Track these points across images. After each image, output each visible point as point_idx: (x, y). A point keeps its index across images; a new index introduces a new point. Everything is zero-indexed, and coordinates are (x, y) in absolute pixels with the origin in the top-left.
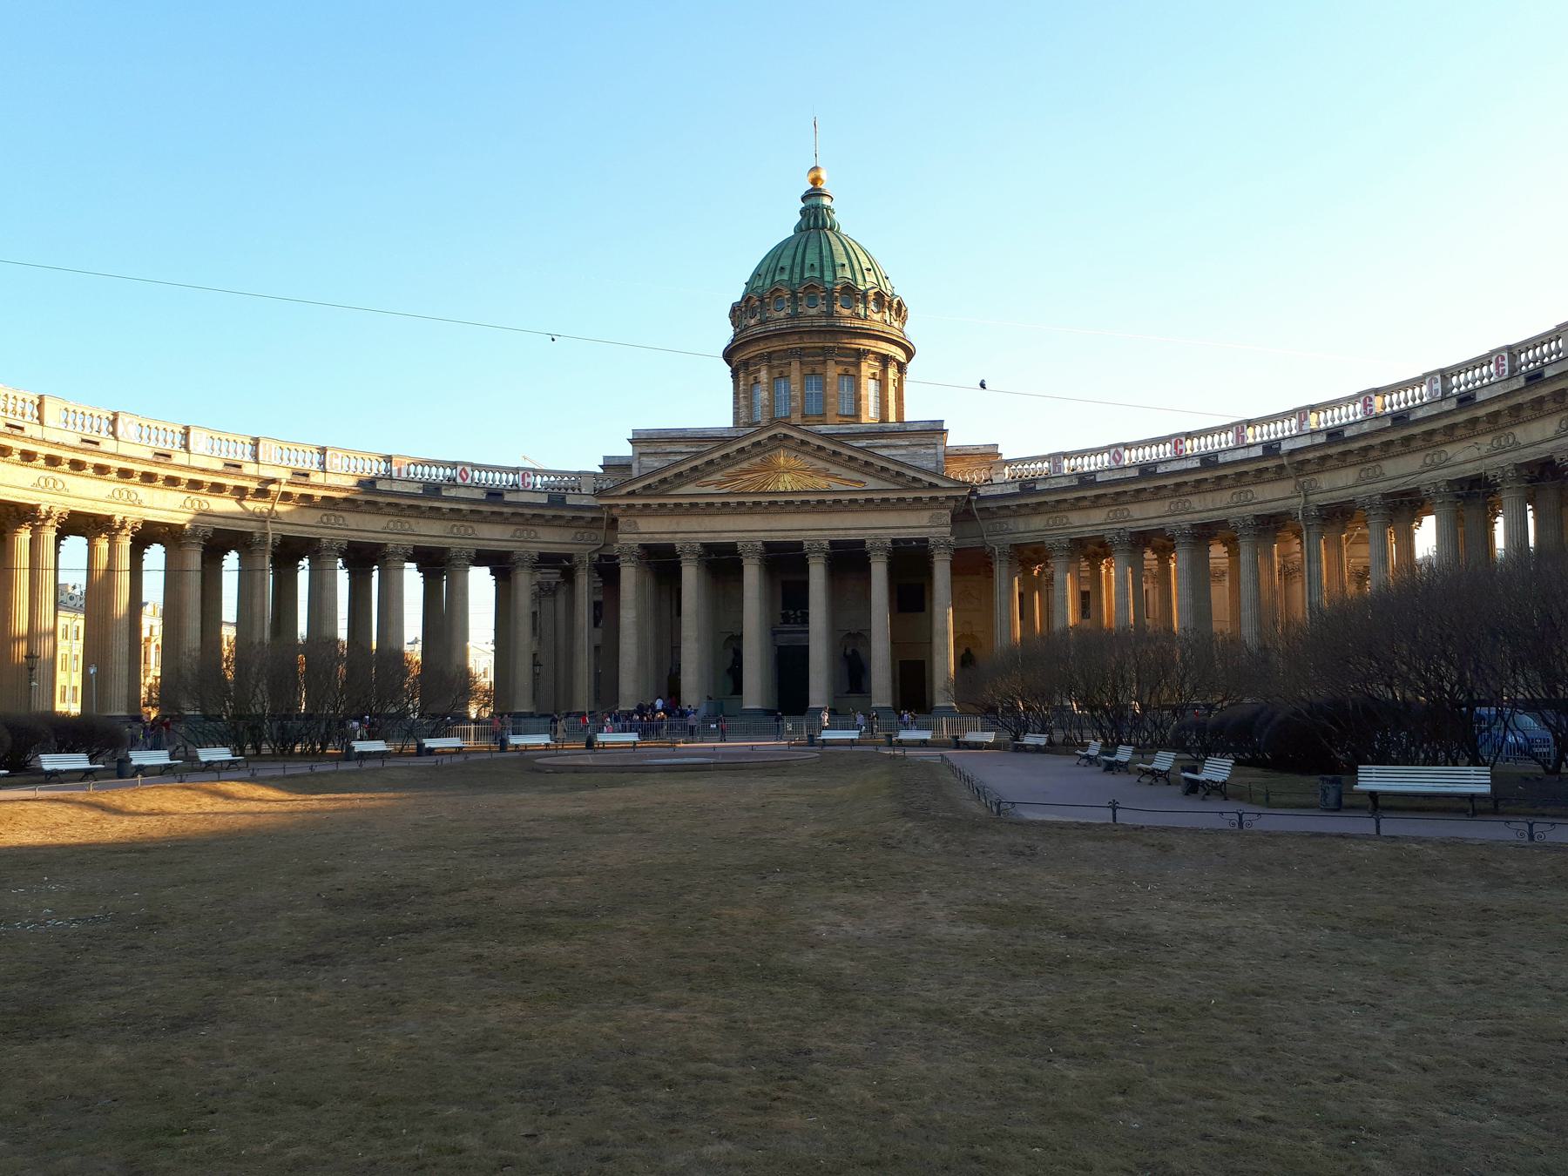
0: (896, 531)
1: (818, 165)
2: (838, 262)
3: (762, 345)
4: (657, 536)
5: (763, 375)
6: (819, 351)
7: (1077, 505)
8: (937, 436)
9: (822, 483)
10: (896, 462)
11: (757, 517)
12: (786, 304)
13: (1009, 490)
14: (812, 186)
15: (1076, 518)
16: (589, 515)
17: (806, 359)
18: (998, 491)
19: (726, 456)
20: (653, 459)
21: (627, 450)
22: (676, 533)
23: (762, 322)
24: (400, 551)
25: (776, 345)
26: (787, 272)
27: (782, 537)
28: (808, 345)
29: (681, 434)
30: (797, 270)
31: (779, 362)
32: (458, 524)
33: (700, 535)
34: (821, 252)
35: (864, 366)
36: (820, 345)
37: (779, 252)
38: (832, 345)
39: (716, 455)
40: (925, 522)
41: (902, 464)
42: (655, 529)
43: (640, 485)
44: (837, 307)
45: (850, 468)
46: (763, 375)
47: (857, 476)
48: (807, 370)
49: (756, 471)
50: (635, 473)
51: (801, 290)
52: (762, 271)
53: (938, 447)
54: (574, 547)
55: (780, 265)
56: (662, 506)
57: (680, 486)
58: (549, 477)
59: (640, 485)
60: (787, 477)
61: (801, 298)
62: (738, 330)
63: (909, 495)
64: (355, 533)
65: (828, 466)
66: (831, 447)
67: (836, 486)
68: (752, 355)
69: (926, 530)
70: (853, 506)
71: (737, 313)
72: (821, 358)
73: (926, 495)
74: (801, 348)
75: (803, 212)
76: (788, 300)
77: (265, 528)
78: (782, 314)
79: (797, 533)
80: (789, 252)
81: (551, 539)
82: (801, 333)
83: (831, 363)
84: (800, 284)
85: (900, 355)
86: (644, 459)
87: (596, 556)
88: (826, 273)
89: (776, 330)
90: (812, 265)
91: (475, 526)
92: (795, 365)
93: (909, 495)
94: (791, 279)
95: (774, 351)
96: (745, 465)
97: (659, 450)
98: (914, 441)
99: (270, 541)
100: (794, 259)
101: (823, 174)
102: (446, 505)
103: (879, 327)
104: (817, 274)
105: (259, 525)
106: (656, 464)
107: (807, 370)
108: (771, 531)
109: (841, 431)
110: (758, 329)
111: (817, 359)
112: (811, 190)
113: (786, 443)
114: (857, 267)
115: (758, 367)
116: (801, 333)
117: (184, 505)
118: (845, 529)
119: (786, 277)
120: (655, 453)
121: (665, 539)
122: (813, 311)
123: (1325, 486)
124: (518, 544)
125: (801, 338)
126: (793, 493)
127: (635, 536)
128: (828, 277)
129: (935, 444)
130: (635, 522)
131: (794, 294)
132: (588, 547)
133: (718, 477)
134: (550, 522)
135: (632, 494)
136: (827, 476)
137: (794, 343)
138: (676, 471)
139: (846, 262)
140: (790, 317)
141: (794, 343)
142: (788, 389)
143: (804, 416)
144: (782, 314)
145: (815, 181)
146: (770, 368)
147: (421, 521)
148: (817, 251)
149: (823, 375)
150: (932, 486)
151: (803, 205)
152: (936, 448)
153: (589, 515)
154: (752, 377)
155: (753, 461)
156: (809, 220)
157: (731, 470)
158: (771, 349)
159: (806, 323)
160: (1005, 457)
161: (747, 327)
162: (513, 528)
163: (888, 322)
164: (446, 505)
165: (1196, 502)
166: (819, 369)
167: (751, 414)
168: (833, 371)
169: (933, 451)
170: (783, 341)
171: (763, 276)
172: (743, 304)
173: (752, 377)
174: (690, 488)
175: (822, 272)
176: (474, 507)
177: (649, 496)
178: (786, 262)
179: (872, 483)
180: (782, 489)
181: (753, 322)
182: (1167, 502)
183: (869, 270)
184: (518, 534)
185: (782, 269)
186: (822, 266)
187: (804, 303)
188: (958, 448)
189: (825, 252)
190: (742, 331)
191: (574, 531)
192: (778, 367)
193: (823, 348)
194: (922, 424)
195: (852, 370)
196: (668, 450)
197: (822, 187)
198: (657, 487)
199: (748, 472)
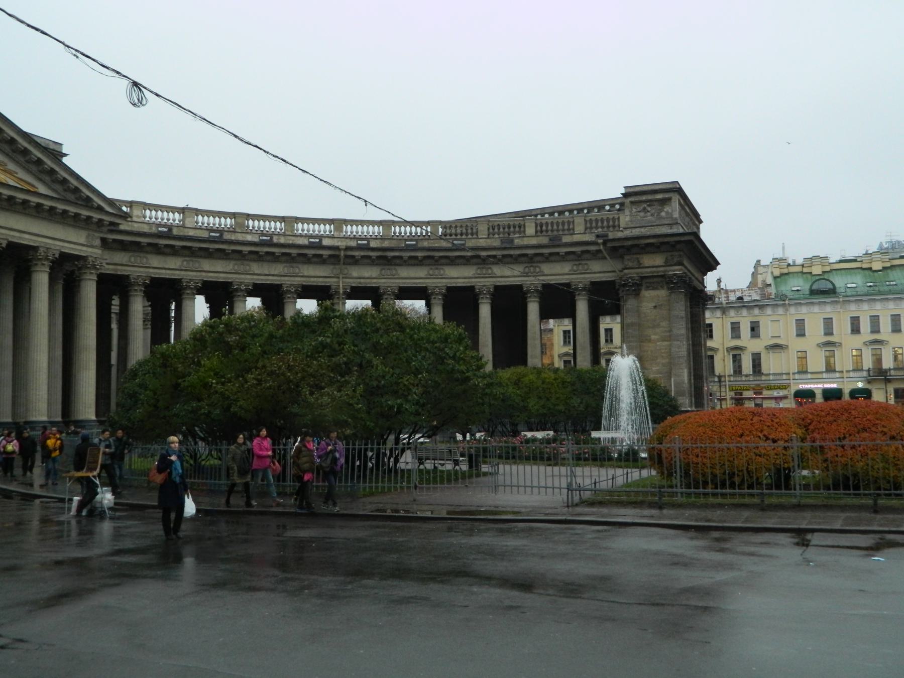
0: (61, 244)
7: (157, 250)
15: (155, 261)
40: (82, 240)
45: (29, 171)
63: (85, 213)
69: (85, 248)
70: (39, 212)
73: (96, 216)
93: (85, 213)
123: (355, 274)
150: (100, 209)
165: (255, 268)
182: (233, 262)
194: (47, 142)
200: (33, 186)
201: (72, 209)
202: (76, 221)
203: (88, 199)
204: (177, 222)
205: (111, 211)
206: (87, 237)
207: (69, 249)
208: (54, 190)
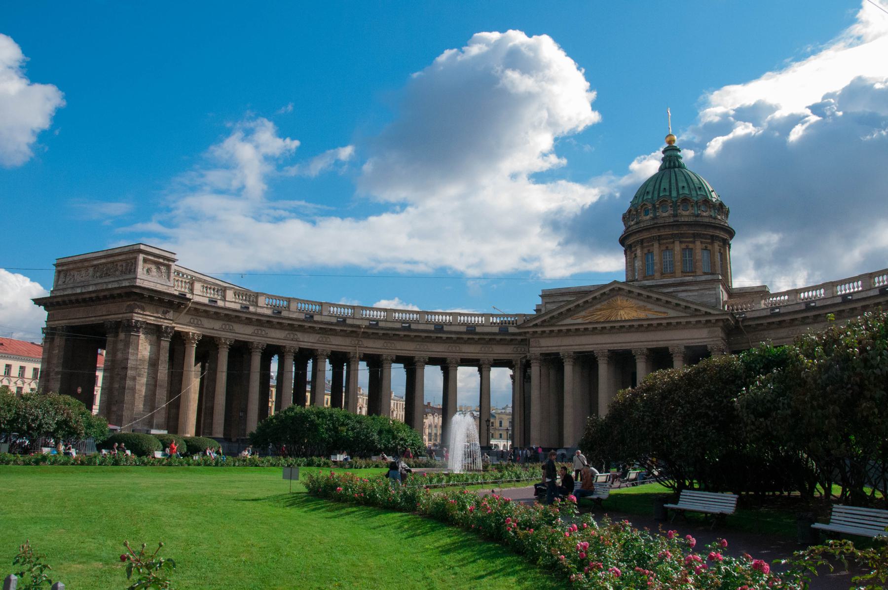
0: (687, 341)
2: (680, 185)
3: (637, 236)
4: (550, 348)
5: (639, 252)
6: (670, 236)
8: (716, 283)
9: (642, 315)
10: (683, 300)
12: (650, 212)
13: (764, 313)
16: (519, 338)
17: (662, 241)
18: (757, 314)
19: (587, 302)
21: (539, 301)
22: (561, 346)
23: (637, 223)
24: (422, 360)
25: (645, 235)
26: (651, 194)
27: (620, 347)
28: (662, 234)
29: (567, 291)
30: (656, 193)
31: (647, 244)
34: (670, 181)
35: (698, 243)
38: (677, 232)
39: (581, 302)
41: (687, 301)
42: (549, 345)
43: (540, 320)
44: (679, 211)
46: (639, 252)
47: (663, 309)
48: (663, 248)
49: (604, 309)
50: (543, 312)
51: (658, 203)
53: (717, 289)
54: (514, 355)
55: (647, 190)
56: (552, 331)
58: (504, 318)
59: (540, 320)
60: (622, 312)
61: (658, 208)
64: (399, 351)
65: (645, 304)
66: (645, 293)
67: (651, 316)
71: (626, 218)
72: (672, 240)
73: (703, 319)
74: (659, 236)
77: (356, 350)
78: (648, 217)
79: (628, 344)
80: (652, 183)
83: (677, 243)
84: (658, 200)
85: (726, 236)
87: (524, 361)
88: (673, 192)
90: (665, 189)
91: (460, 346)
93: (693, 320)
94: (652, 197)
95: (645, 238)
96: (598, 306)
97: (555, 300)
98: (702, 287)
99: (358, 356)
100: (654, 187)
102: (444, 336)
103: (707, 220)
104: (667, 194)
105: (354, 348)
107: (663, 248)
108: (612, 343)
109: (658, 283)
110: (634, 227)
111: (669, 241)
112: (668, 147)
113: (620, 292)
114: (692, 186)
116: (659, 228)
117: (318, 340)
118: (657, 341)
119: (650, 197)
120: (554, 302)
121: (554, 350)
122: (664, 214)
124: (483, 355)
125: (659, 230)
126: (625, 321)
127: (539, 349)
128: (674, 194)
129: (715, 288)
130: (539, 341)
131: (654, 206)
132: (519, 355)
133: (583, 314)
134: (501, 342)
135: (536, 325)
136: (645, 310)
137: (655, 233)
139: (685, 185)
140: (653, 219)
141: (655, 233)
142: (653, 260)
143: (662, 274)
144: (648, 217)
145: (670, 142)
146: (642, 248)
148: (668, 180)
149: (673, 250)
150: (707, 314)
151: (663, 156)
152: (715, 290)
153: (519, 338)
154: (633, 254)
155: (603, 304)
157: (591, 309)
159: (661, 221)
160: (771, 292)
161: (630, 226)
163: (713, 215)
164: (444, 336)
166: (670, 246)
167: (634, 275)
168: (677, 247)
169: (714, 292)
173: (633, 254)
174: (568, 321)
175: (670, 192)
176: (459, 336)
177: (544, 326)
178: (650, 189)
179: (672, 313)
180: (619, 319)
181: (633, 223)
183: (700, 188)
184: (483, 349)
185: (648, 193)
186: (670, 188)
187: (660, 211)
188: (741, 289)
189: (673, 181)
191: (513, 346)
192: (648, 246)
193: (672, 234)
195: (691, 246)
196: (561, 300)
197: (674, 145)
198: (549, 321)
199: (601, 310)
200: (665, 313)
201: (683, 320)
203: (696, 310)
204: (823, 295)
208: (680, 311)
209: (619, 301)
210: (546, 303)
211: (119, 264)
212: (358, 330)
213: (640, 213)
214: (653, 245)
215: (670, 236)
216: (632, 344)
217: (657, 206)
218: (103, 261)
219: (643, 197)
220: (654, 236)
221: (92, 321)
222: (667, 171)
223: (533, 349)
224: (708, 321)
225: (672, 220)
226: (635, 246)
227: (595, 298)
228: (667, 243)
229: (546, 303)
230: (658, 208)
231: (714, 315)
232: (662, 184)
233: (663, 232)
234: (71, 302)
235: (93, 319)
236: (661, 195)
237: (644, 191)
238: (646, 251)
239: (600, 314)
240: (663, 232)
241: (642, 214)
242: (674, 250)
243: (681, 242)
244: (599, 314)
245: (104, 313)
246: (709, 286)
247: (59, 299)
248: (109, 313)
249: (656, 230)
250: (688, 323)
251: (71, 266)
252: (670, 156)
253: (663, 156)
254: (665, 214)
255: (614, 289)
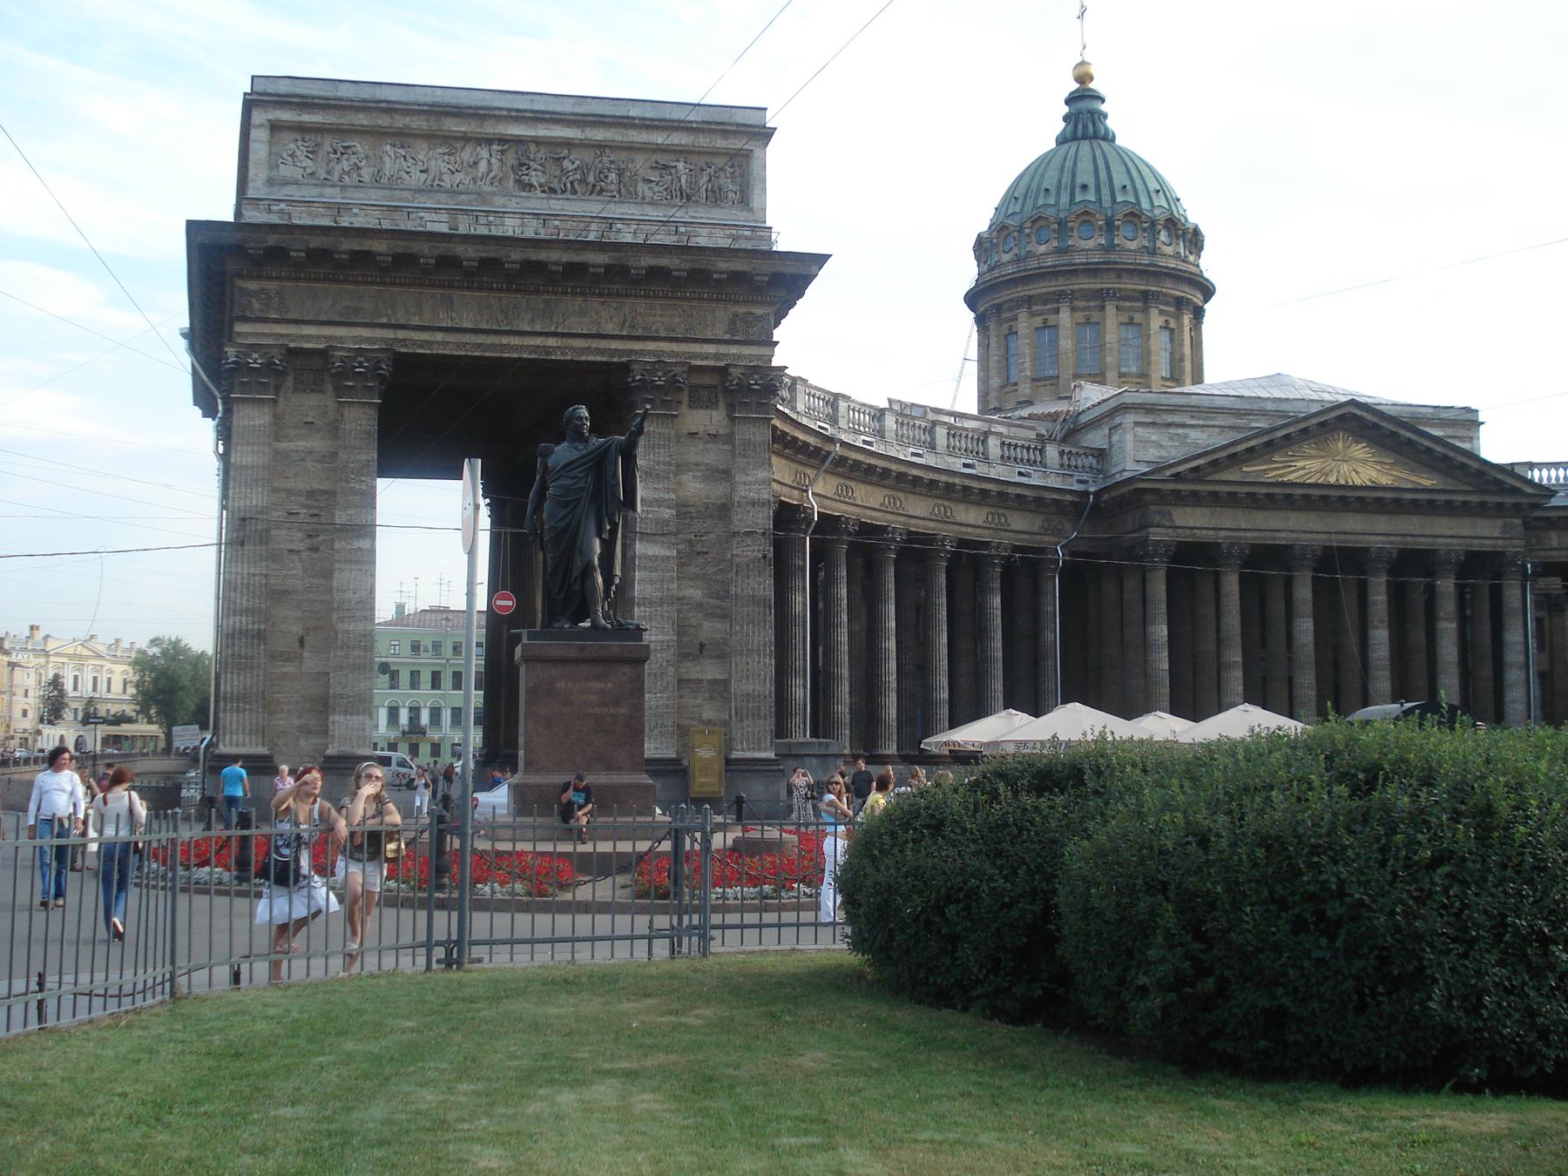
0: (1468, 541)
1: (1086, 60)
3: (1061, 281)
5: (1065, 318)
9: (1385, 481)
11: (1313, 515)
14: (1076, 86)
20: (1150, 430)
22: (1221, 529)
23: (1060, 251)
26: (1092, 190)
30: (1105, 191)
31: (1084, 304)
32: (939, 502)
33: (1248, 534)
36: (1143, 288)
37: (1069, 164)
42: (1195, 522)
46: (1065, 318)
49: (1311, 457)
51: (1120, 216)
52: (1050, 181)
55: (1079, 181)
57: (1226, 468)
60: (1345, 468)
62: (1006, 258)
63: (1490, 499)
68: (1044, 290)
72: (1139, 304)
74: (1121, 290)
75: (1066, 118)
76: (1101, 228)
78: (1091, 244)
81: (1021, 524)
82: (1120, 272)
83: (1154, 312)
86: (1139, 429)
89: (1087, 264)
90: (1125, 187)
91: (952, 505)
92: (1110, 309)
95: (1081, 290)
97: (1158, 420)
101: (1094, 70)
106: (1154, 438)
107: (1124, 319)
111: (1135, 304)
115: (1048, 307)
116: (1120, 272)
119: (1091, 197)
120: (1154, 424)
121: (1207, 536)
122: (1133, 245)
125: (1119, 277)
127: (1170, 531)
128: (1145, 205)
138: (1231, 451)
140: (1102, 248)
143: (1121, 375)
144: (1091, 244)
145: (1083, 78)
146: (1073, 309)
147: (911, 497)
150: (1514, 491)
151: (1066, 109)
156: (1085, 127)
158: (1076, 287)
162: (987, 510)
168: (1156, 321)
170: (1095, 277)
171: (1053, 191)
172: (1028, 224)
173: (1038, 321)
178: (1086, 176)
180: (1343, 482)
181: (1043, 249)
185: (1084, 187)
186: (1135, 189)
187: (1120, 233)
190: (1018, 260)
192: (1083, 309)
197: (1092, 85)
201: (1474, 499)
202: (1483, 510)
205: (1530, 491)
206: (1505, 526)
207: (1476, 545)
209: (1340, 444)
210: (1137, 424)
211: (641, 163)
212: (828, 447)
213: (1072, 229)
214: (1102, 308)
215: (1137, 295)
216: (1367, 538)
217: (1117, 223)
218: (559, 132)
219: (1072, 195)
220: (1109, 289)
221: (547, 349)
222: (1066, 146)
223: (1158, 530)
224: (1516, 506)
225: (1146, 260)
226: (1058, 301)
227: (1305, 431)
228: (1132, 309)
229: (1137, 424)
230: (1118, 228)
231: (1530, 494)
232: (1114, 175)
233: (1128, 285)
234: (448, 263)
235: (551, 342)
236: (1120, 198)
237: (1066, 179)
238: (1080, 316)
239: (1304, 468)
240: (1128, 285)
241: (1075, 233)
242: (1148, 328)
243: (1161, 312)
244: (1307, 468)
245: (609, 328)
246: (1460, 432)
247: (469, 253)
248: (639, 332)
249: (1113, 275)
250: (1482, 504)
251: (362, 120)
252: (1080, 113)
253: (1066, 109)
254: (1130, 242)
255: (1341, 418)
